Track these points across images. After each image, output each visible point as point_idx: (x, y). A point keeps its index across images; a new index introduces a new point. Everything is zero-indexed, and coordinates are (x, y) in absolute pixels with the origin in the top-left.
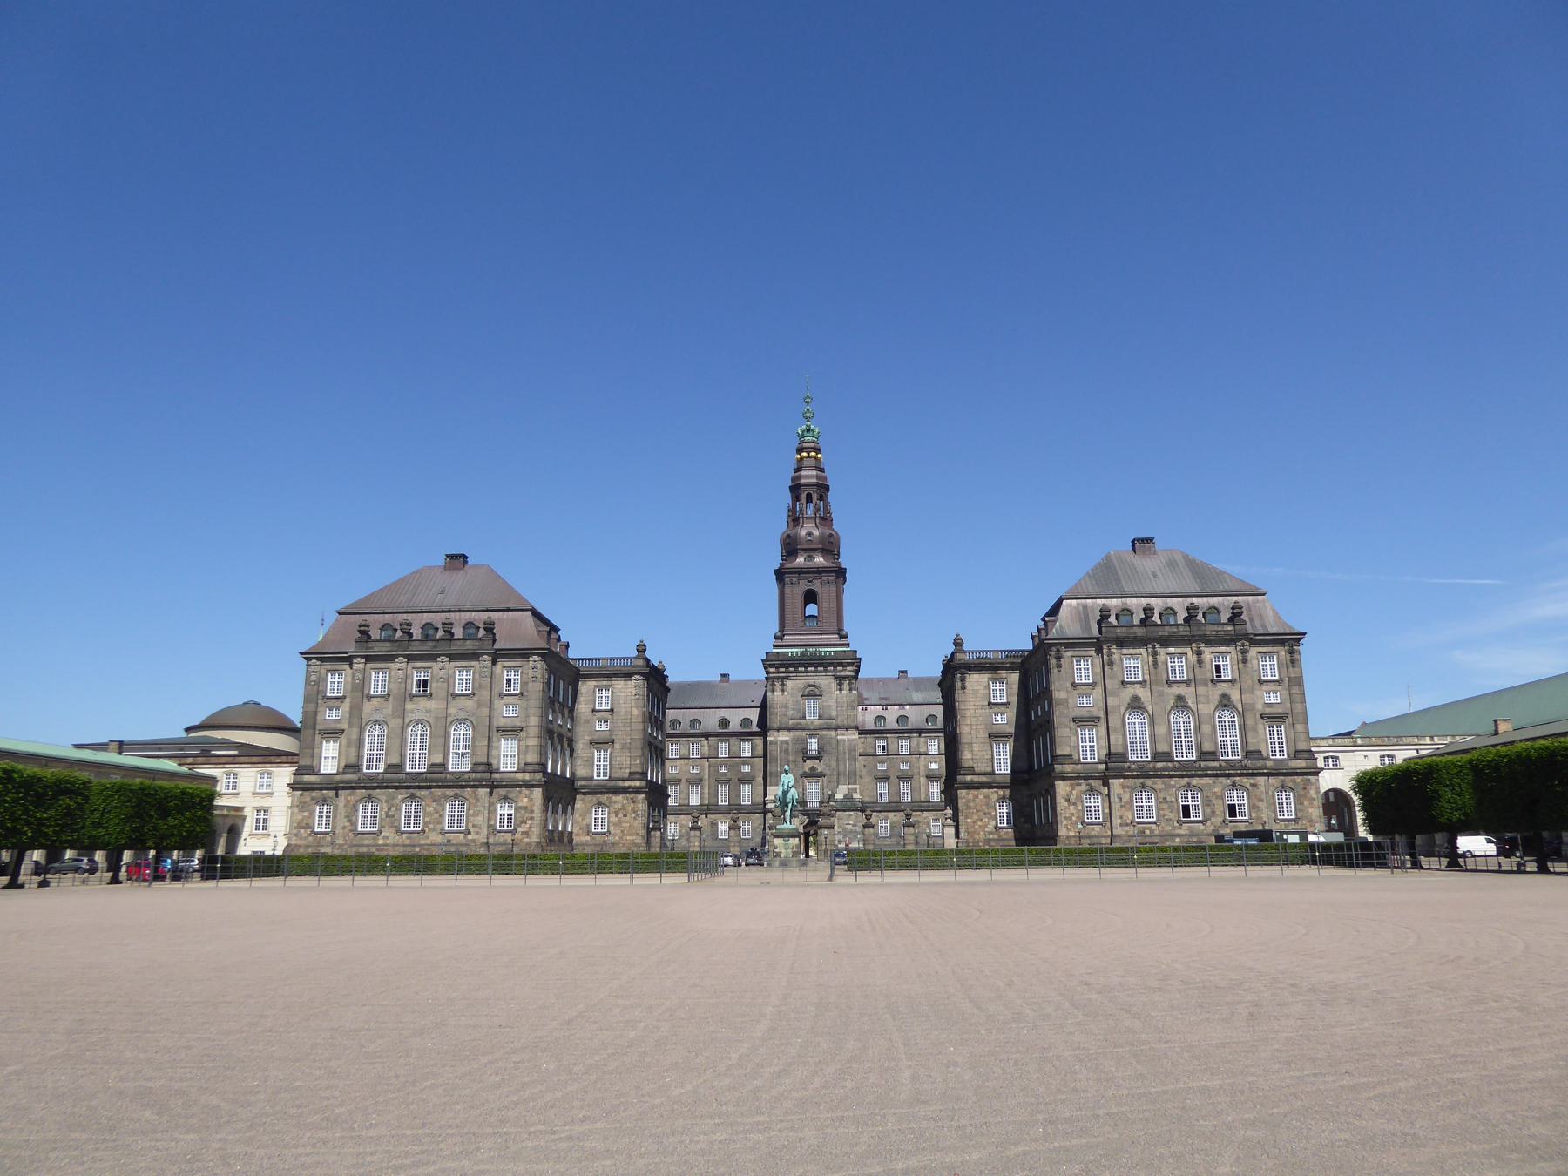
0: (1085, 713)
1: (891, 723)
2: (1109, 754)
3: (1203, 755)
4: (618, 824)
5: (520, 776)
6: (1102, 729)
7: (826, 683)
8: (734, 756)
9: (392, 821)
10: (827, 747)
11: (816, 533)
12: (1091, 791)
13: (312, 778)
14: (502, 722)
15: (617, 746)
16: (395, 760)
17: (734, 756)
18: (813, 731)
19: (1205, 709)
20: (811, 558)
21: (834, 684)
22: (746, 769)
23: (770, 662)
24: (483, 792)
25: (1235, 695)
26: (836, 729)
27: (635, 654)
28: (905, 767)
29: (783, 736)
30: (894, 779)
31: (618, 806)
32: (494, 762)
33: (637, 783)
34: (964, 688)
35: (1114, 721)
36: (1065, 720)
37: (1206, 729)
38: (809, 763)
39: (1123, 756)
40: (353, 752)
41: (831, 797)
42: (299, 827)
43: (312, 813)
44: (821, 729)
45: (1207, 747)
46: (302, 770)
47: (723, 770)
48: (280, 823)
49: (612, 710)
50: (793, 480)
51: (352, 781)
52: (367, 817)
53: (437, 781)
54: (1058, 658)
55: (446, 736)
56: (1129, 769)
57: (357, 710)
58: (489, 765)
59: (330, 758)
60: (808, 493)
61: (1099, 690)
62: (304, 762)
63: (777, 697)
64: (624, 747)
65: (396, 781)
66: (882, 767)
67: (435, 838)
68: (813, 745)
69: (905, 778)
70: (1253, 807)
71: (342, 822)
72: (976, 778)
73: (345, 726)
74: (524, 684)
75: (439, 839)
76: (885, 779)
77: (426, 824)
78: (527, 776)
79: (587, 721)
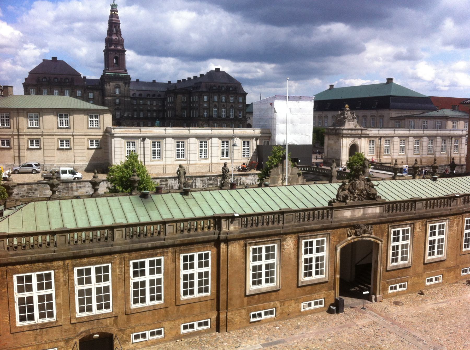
3: (227, 116)
7: (121, 84)
11: (117, 38)
19: (228, 108)
20: (117, 47)
25: (234, 105)
28: (141, 108)
29: (110, 98)
35: (211, 109)
37: (228, 112)
38: (117, 107)
39: (212, 116)
41: (123, 115)
49: (93, 98)
54: (201, 95)
63: (107, 87)
68: (118, 101)
69: (142, 110)
74: (82, 94)
76: (135, 110)
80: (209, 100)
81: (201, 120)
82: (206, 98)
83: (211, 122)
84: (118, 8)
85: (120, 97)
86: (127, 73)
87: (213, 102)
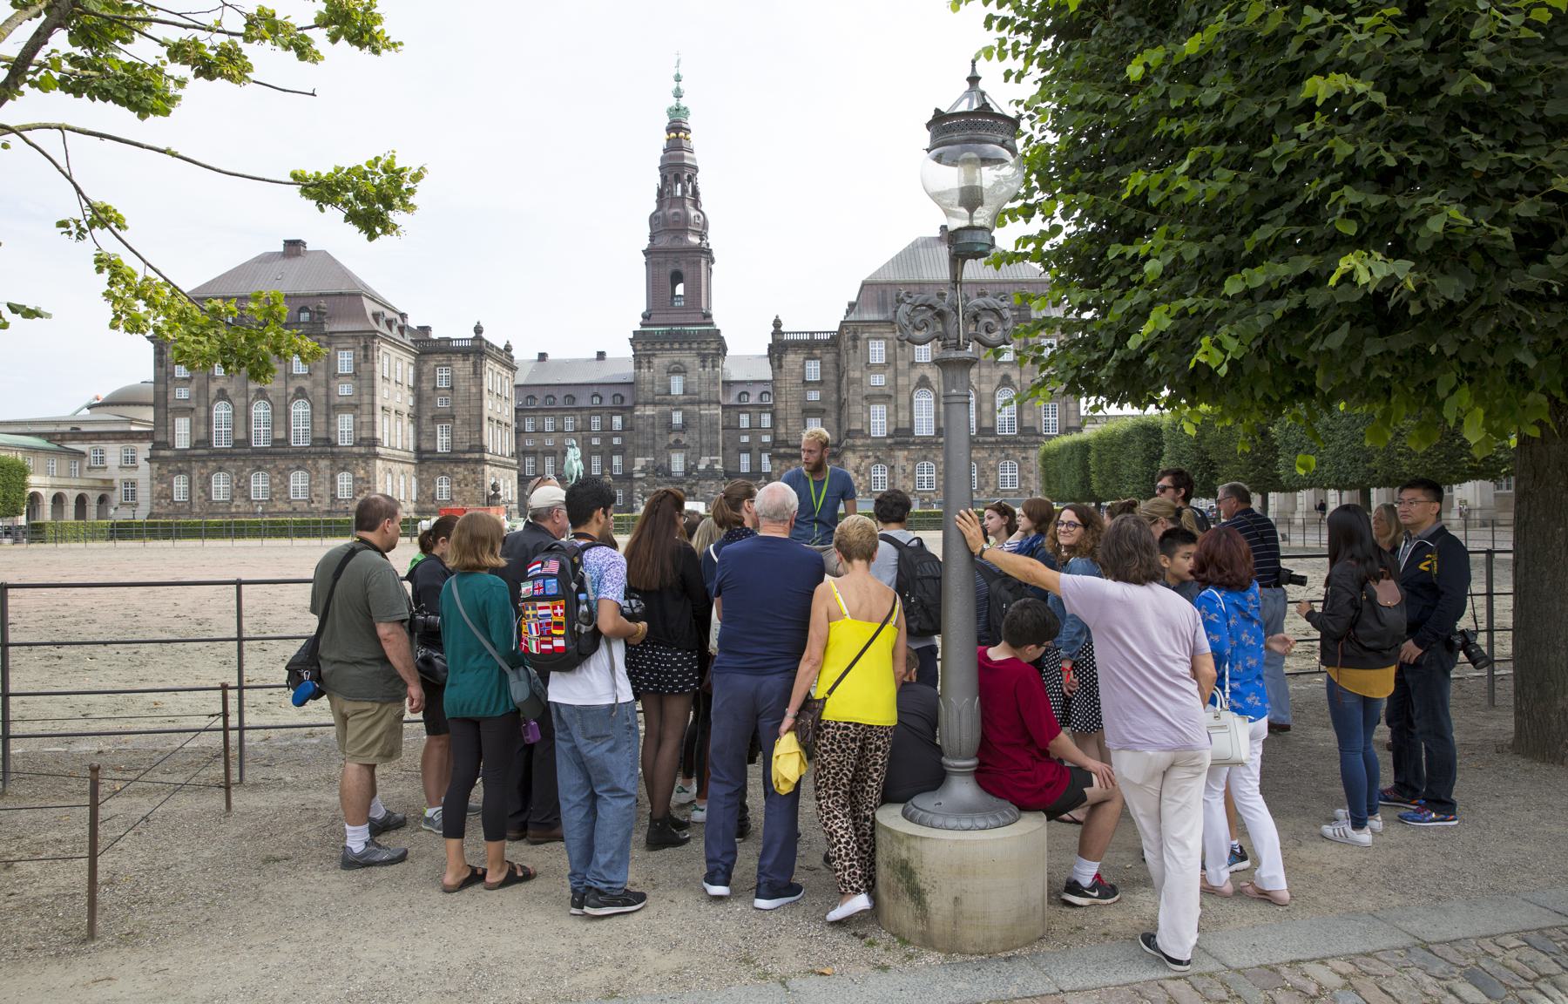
0: (876, 391)
1: (753, 400)
2: (896, 430)
4: (460, 493)
5: (356, 450)
6: (892, 407)
7: (689, 359)
8: (607, 431)
9: (241, 490)
10: (691, 421)
12: (879, 460)
13: (168, 453)
14: (338, 400)
15: (458, 422)
16: (241, 435)
17: (607, 431)
18: (677, 405)
19: (986, 389)
21: (697, 361)
22: (616, 441)
23: (637, 339)
24: (323, 463)
26: (700, 402)
27: (473, 335)
29: (650, 411)
30: (755, 451)
31: (460, 477)
32: (333, 437)
33: (477, 456)
34: (780, 366)
35: (903, 399)
36: (859, 398)
37: (986, 407)
38: (673, 438)
39: (910, 431)
40: (202, 430)
41: (695, 466)
42: (160, 497)
43: (171, 485)
44: (685, 403)
45: (986, 423)
46: (156, 446)
47: (595, 442)
48: (144, 494)
50: (662, 159)
51: (203, 453)
52: (220, 486)
53: (280, 454)
55: (287, 413)
56: (914, 443)
57: (202, 391)
58: (328, 440)
59: (182, 433)
60: (677, 171)
61: (892, 369)
62: (160, 438)
64: (463, 423)
65: (242, 453)
66: (745, 439)
67: (281, 506)
68: (677, 418)
70: (1023, 478)
71: (197, 492)
72: (789, 451)
73: (193, 405)
74: (357, 365)
75: (286, 507)
76: (747, 449)
77: (272, 494)
78: (363, 450)
79: (429, 398)
80: (890, 362)
81: (853, 448)
82: (877, 351)
83: (901, 454)
84: (691, 122)
85: (685, 403)
86: (712, 324)
87: (913, 364)
